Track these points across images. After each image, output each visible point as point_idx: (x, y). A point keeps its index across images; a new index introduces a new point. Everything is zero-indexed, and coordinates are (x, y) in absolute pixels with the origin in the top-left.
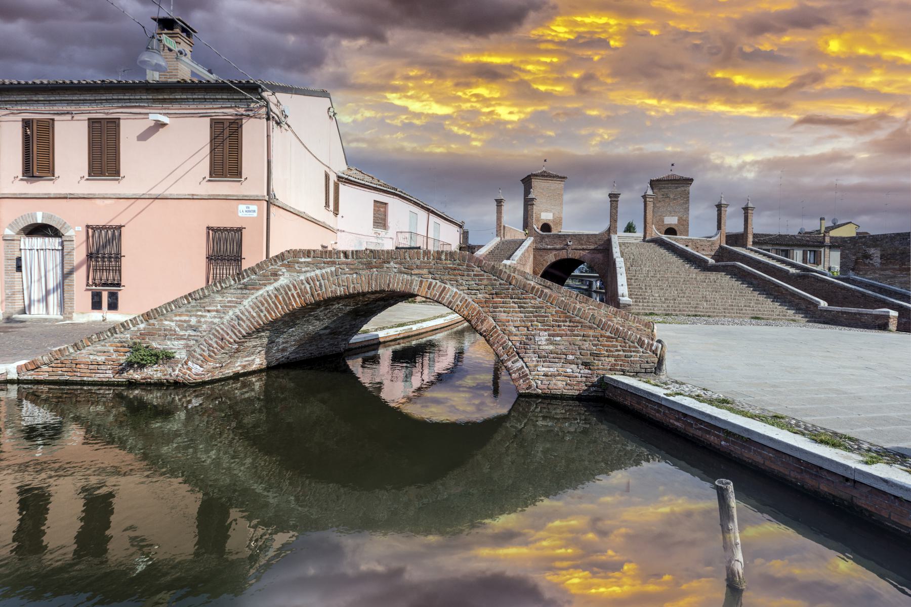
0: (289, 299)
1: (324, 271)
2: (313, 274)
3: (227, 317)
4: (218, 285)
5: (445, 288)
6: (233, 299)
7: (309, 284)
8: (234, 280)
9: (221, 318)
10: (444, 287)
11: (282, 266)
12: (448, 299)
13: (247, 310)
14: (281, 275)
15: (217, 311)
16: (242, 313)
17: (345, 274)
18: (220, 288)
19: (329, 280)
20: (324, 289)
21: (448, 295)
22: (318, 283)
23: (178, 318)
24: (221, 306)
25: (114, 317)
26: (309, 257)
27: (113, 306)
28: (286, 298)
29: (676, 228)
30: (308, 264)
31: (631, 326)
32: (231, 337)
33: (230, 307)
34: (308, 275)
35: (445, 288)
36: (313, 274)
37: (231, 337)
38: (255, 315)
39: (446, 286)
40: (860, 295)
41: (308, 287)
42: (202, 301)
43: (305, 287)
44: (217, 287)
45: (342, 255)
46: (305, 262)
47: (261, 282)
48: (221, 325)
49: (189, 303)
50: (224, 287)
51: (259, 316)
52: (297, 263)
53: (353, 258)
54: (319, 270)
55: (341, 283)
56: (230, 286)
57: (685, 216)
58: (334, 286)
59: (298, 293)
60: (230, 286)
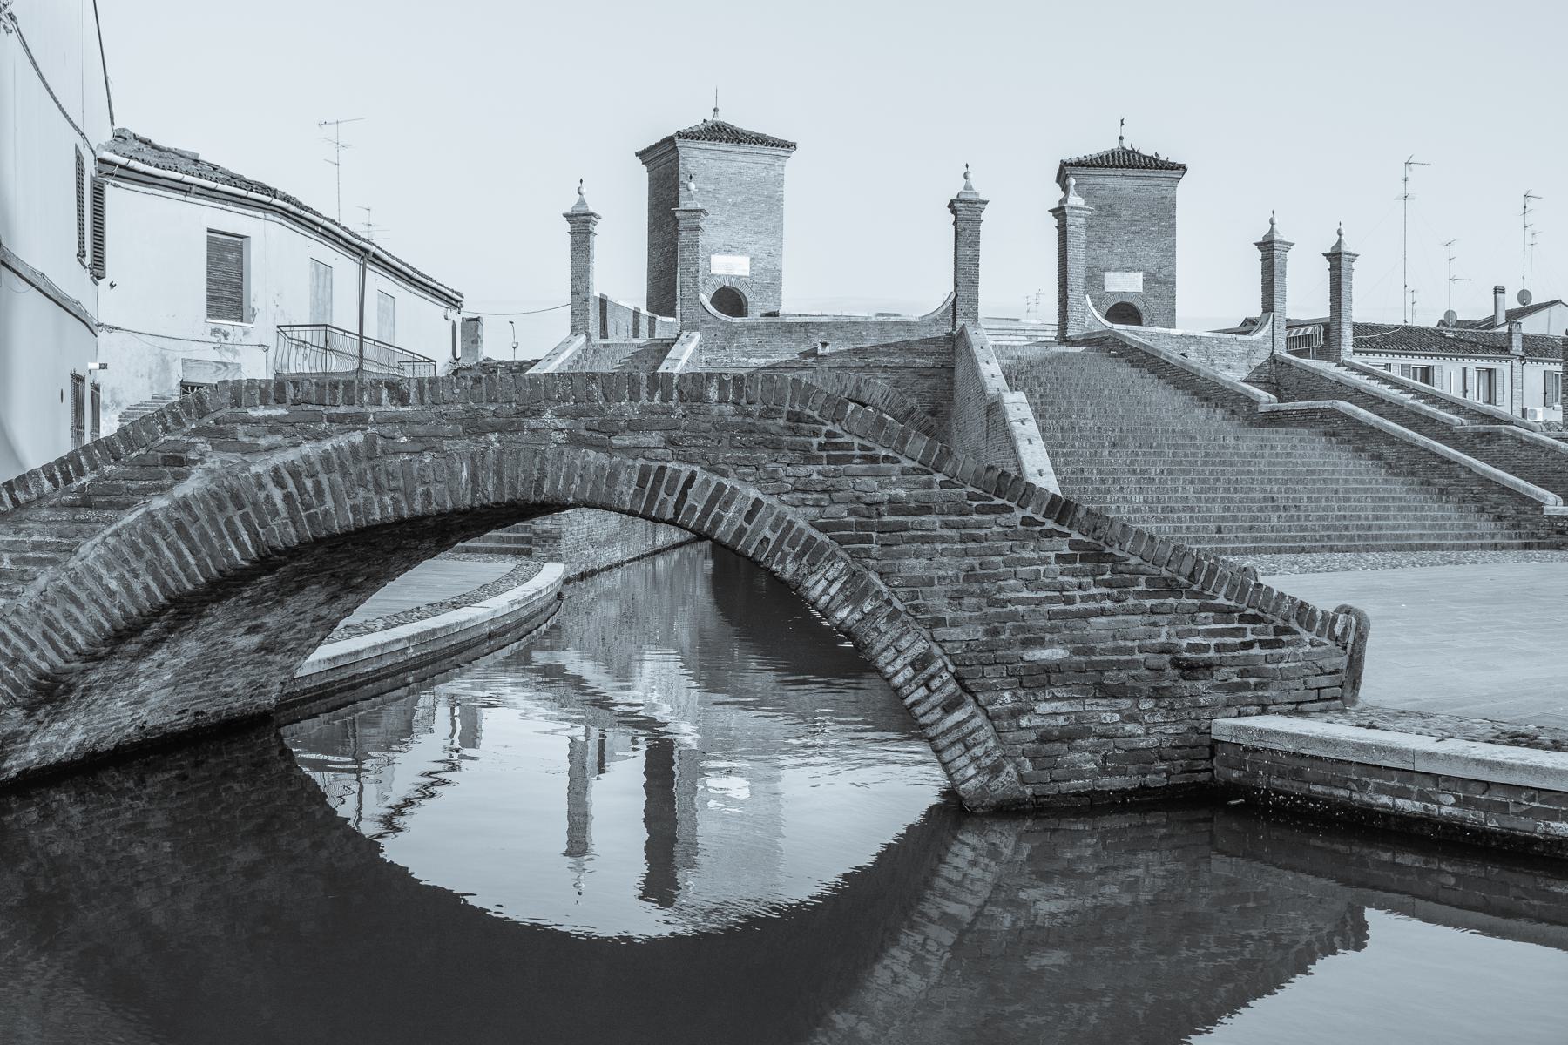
0: (221, 536)
1: (328, 445)
3: (31, 593)
5: (721, 487)
6: (48, 539)
8: (52, 478)
10: (719, 484)
11: (197, 432)
12: (731, 523)
13: (90, 570)
14: (194, 462)
16: (76, 581)
17: (397, 453)
19: (345, 473)
20: (330, 504)
21: (733, 509)
22: (309, 484)
24: (13, 561)
26: (280, 401)
28: (212, 534)
30: (274, 426)
33: (40, 562)
34: (278, 459)
35: (721, 487)
36: (292, 455)
37: (42, 657)
38: (113, 585)
39: (724, 481)
41: (277, 495)
43: (268, 497)
45: (385, 394)
46: (267, 419)
47: (133, 485)
51: (128, 588)
53: (422, 402)
54: (313, 444)
55: (383, 480)
56: (41, 497)
58: (361, 492)
59: (245, 518)
60: (41, 497)
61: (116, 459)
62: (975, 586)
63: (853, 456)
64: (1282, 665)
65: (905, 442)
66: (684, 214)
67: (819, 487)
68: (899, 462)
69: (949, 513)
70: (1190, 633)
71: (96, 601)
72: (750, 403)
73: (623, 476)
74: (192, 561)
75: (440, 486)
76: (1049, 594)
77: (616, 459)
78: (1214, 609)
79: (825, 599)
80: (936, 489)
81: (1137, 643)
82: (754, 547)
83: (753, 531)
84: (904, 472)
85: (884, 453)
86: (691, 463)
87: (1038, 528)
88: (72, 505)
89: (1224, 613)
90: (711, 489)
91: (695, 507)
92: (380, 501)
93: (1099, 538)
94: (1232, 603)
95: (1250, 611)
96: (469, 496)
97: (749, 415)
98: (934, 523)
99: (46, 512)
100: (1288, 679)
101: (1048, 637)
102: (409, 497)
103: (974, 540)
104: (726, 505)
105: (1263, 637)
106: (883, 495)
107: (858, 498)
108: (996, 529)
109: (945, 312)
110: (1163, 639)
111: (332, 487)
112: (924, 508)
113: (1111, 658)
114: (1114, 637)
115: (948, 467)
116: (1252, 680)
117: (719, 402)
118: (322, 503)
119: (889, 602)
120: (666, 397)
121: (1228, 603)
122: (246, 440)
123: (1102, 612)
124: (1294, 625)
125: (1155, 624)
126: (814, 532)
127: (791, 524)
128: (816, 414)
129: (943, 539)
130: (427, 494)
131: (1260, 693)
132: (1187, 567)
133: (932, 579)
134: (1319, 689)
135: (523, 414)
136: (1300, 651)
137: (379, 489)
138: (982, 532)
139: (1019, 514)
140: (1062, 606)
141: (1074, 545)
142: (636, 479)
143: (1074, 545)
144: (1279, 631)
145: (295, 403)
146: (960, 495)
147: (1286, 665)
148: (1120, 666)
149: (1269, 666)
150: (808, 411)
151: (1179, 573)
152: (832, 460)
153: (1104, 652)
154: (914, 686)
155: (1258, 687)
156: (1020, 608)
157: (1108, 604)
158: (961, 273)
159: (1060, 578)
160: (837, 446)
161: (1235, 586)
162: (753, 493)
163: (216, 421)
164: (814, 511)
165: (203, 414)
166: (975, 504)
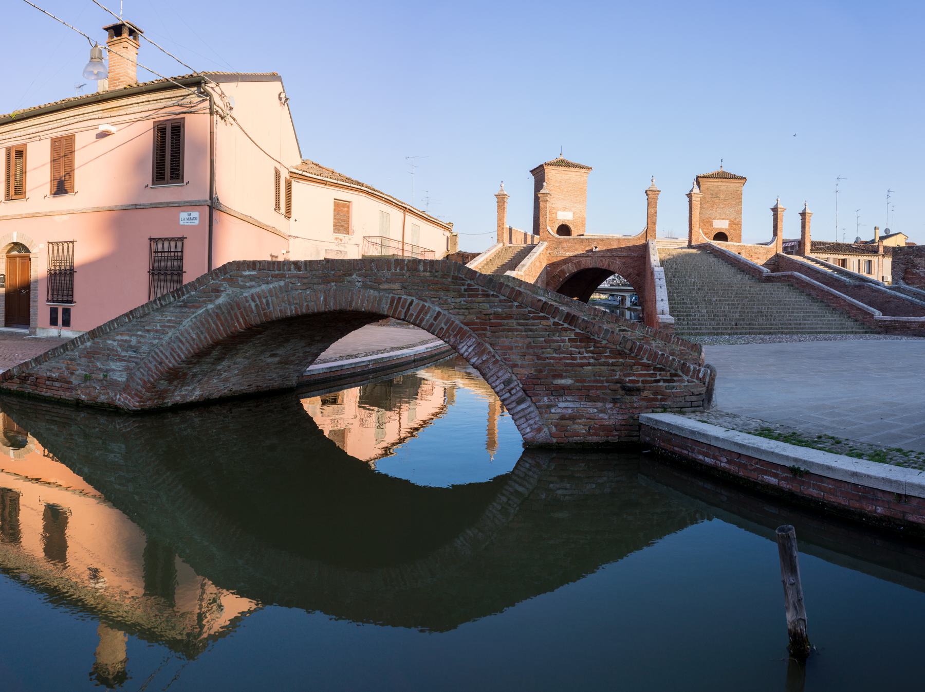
0: (232, 319)
1: (271, 286)
2: (258, 289)
3: (167, 338)
4: (158, 302)
5: (424, 306)
6: (172, 319)
7: (255, 302)
8: (173, 296)
9: (160, 339)
10: (423, 305)
11: (224, 280)
12: (428, 321)
13: (186, 330)
14: (223, 291)
15: (157, 331)
16: (182, 334)
17: (296, 290)
18: (159, 306)
19: (277, 297)
20: (272, 309)
21: (429, 315)
22: (264, 301)
23: (119, 337)
24: (161, 326)
25: (68, 334)
26: (254, 269)
27: (67, 323)
28: (229, 318)
29: (727, 234)
30: (252, 278)
31: (673, 350)
32: (170, 362)
33: (169, 327)
34: (253, 291)
35: (424, 306)
36: (258, 289)
38: (194, 336)
39: (425, 304)
40: (907, 303)
41: (253, 305)
42: (142, 320)
43: (250, 305)
44: (157, 305)
45: (292, 267)
47: (201, 299)
48: (161, 347)
49: (130, 321)
50: (163, 304)
52: (241, 276)
53: (306, 270)
56: (170, 303)
57: (737, 220)
58: (283, 304)
59: (241, 313)
60: (170, 303)
61: (196, 290)
62: (531, 351)
63: (478, 294)
64: (673, 391)
65: (501, 288)
66: (541, 195)
67: (464, 307)
68: (499, 297)
69: (520, 319)
70: (630, 375)
71: (188, 342)
72: (437, 272)
73: (384, 301)
74: (222, 328)
75: (313, 303)
76: (566, 355)
77: (382, 294)
78: (643, 365)
79: (466, 354)
80: (514, 309)
81: (605, 378)
82: (437, 332)
83: (437, 325)
84: (500, 301)
85: (492, 293)
86: (411, 296)
87: (561, 327)
88: (181, 306)
89: (647, 367)
90: (420, 307)
91: (413, 314)
92: (290, 308)
93: (588, 332)
94: (650, 362)
95: (658, 366)
96: (324, 307)
97: (436, 276)
98: (513, 323)
99: (172, 309)
100: (676, 397)
101: (564, 374)
102: (301, 306)
103: (531, 331)
104: (426, 313)
105: (665, 378)
106: (492, 311)
107: (481, 312)
108: (541, 326)
109: (643, 235)
110: (617, 377)
111: (272, 302)
112: (509, 317)
113: (593, 384)
114: (594, 375)
115: (520, 299)
116: (659, 397)
117: (424, 271)
118: (269, 308)
119: (494, 356)
120: (402, 269)
121: (648, 362)
122: (242, 283)
123: (589, 364)
124: (681, 373)
125: (613, 370)
126: (462, 326)
127: (453, 322)
128: (463, 276)
129: (517, 330)
130: (308, 306)
131: (663, 403)
132: (629, 345)
133: (512, 347)
134: (691, 402)
135: (345, 275)
136: (683, 384)
137: (290, 304)
138: (535, 328)
139: (552, 320)
140: (571, 361)
141: (576, 334)
142: (389, 302)
143: (576, 334)
144: (672, 375)
145: (260, 270)
146: (525, 311)
147: (675, 391)
148: (597, 388)
149: (668, 391)
150: (460, 275)
151: (625, 348)
152: (470, 296)
153: (589, 381)
154: (504, 392)
155: (661, 400)
156: (552, 361)
157: (592, 361)
158: (649, 219)
159: (570, 349)
160: (472, 290)
161: (651, 355)
162: (437, 309)
163: (230, 276)
164: (462, 317)
165: (225, 273)
166: (532, 315)
